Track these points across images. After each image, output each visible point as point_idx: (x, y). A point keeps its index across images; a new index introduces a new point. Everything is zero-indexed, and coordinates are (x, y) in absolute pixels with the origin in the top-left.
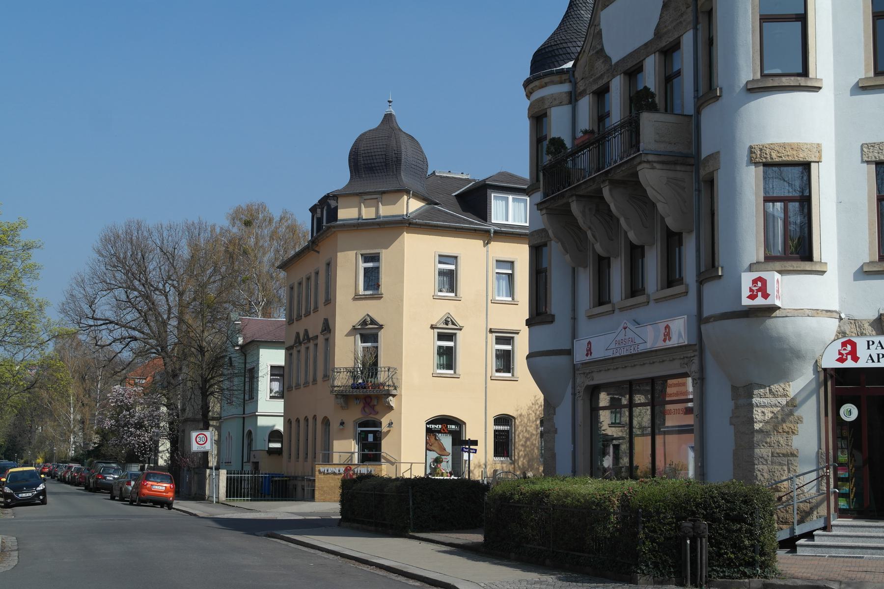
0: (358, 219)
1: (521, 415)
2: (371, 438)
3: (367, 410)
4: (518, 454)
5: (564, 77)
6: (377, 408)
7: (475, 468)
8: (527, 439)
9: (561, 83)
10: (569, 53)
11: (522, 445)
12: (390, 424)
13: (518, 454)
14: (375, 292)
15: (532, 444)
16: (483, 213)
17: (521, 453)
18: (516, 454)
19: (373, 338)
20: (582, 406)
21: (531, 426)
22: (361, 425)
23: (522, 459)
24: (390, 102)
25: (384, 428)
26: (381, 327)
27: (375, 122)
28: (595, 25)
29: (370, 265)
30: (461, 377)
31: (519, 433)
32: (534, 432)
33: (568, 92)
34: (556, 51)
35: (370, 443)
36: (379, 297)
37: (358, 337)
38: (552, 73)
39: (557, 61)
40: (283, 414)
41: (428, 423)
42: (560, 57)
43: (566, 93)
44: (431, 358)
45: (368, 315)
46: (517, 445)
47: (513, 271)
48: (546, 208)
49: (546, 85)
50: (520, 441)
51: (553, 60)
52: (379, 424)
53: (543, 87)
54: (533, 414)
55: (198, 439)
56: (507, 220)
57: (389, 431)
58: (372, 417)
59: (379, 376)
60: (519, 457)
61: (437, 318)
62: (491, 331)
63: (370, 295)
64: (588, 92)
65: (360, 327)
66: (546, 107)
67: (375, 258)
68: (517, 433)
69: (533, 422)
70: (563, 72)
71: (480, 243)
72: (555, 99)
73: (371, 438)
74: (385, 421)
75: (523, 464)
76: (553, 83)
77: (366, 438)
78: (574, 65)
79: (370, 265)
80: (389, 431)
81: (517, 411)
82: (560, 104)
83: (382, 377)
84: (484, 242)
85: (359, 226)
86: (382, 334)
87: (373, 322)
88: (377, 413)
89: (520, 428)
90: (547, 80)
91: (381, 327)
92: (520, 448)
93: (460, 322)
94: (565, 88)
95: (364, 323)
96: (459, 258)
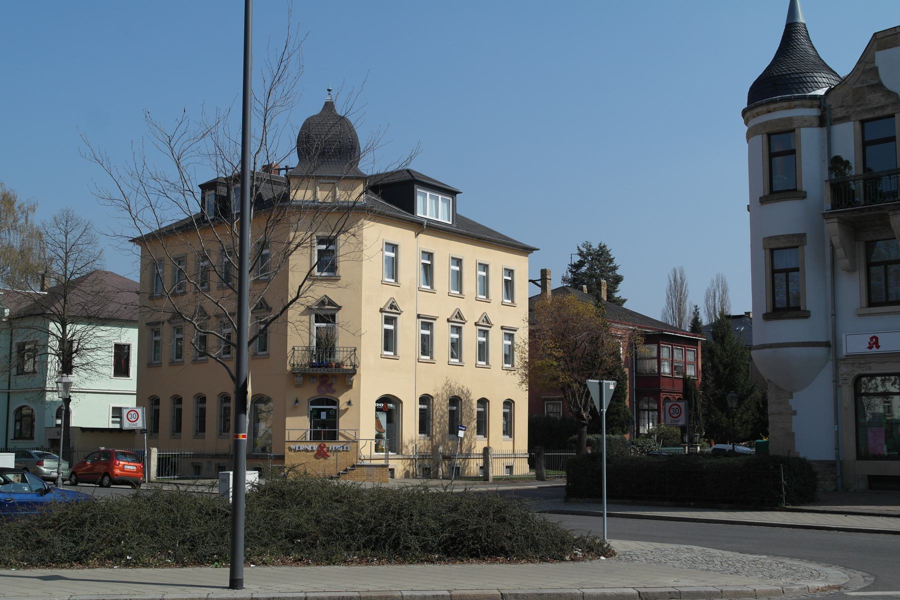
0: (314, 201)
1: (437, 395)
2: (323, 416)
3: (323, 388)
4: (436, 430)
5: (816, 103)
6: (334, 387)
7: (409, 443)
8: (442, 417)
9: (811, 107)
10: (816, 82)
11: (439, 422)
12: (349, 403)
13: (436, 430)
14: (331, 274)
15: (445, 421)
16: (410, 207)
17: (438, 429)
18: (434, 430)
19: (329, 318)
20: (847, 393)
21: (444, 405)
22: (312, 403)
23: (438, 435)
24: (329, 90)
25: (342, 405)
26: (340, 308)
27: (316, 109)
28: (866, 63)
29: (324, 247)
30: (400, 358)
31: (437, 411)
32: (446, 410)
33: (818, 116)
34: (804, 79)
35: (323, 420)
36: (337, 279)
37: (313, 316)
38: (805, 97)
39: (801, 88)
40: (135, 392)
41: (377, 402)
42: (808, 84)
43: (815, 116)
44: (379, 340)
45: (326, 296)
46: (434, 422)
47: (432, 262)
48: (838, 218)
49: (795, 107)
50: (436, 419)
51: (801, 86)
52: (335, 403)
53: (790, 109)
54: (445, 394)
55: (129, 416)
56: (437, 217)
57: (347, 409)
58: (329, 395)
59: (336, 356)
60: (436, 434)
61: (383, 302)
62: (419, 316)
63: (325, 276)
64: (852, 119)
65: (317, 307)
66: (795, 127)
67: (330, 241)
68: (434, 411)
69: (445, 401)
70: (815, 97)
71: (412, 233)
72: (805, 121)
73: (323, 416)
74: (343, 400)
75: (439, 441)
76: (803, 106)
77: (319, 416)
78: (827, 93)
79: (324, 247)
80: (347, 409)
81: (435, 390)
82: (811, 126)
83: (340, 357)
84: (415, 233)
85: (316, 208)
86: (339, 316)
87: (331, 303)
88: (334, 391)
89: (437, 407)
90: (797, 103)
91: (340, 308)
92: (437, 425)
93: (401, 308)
94: (814, 112)
95: (322, 303)
96: (399, 247)
